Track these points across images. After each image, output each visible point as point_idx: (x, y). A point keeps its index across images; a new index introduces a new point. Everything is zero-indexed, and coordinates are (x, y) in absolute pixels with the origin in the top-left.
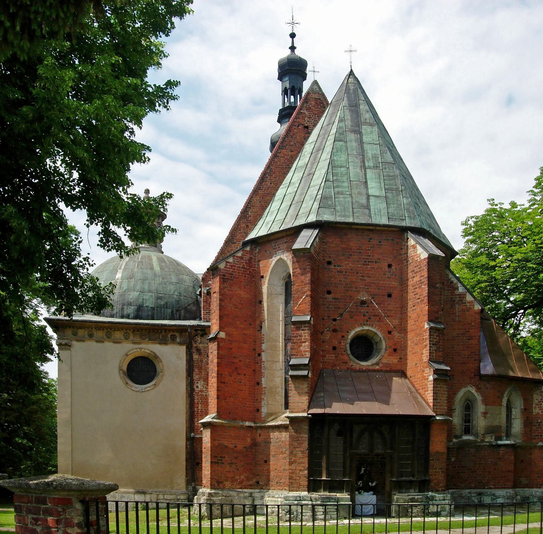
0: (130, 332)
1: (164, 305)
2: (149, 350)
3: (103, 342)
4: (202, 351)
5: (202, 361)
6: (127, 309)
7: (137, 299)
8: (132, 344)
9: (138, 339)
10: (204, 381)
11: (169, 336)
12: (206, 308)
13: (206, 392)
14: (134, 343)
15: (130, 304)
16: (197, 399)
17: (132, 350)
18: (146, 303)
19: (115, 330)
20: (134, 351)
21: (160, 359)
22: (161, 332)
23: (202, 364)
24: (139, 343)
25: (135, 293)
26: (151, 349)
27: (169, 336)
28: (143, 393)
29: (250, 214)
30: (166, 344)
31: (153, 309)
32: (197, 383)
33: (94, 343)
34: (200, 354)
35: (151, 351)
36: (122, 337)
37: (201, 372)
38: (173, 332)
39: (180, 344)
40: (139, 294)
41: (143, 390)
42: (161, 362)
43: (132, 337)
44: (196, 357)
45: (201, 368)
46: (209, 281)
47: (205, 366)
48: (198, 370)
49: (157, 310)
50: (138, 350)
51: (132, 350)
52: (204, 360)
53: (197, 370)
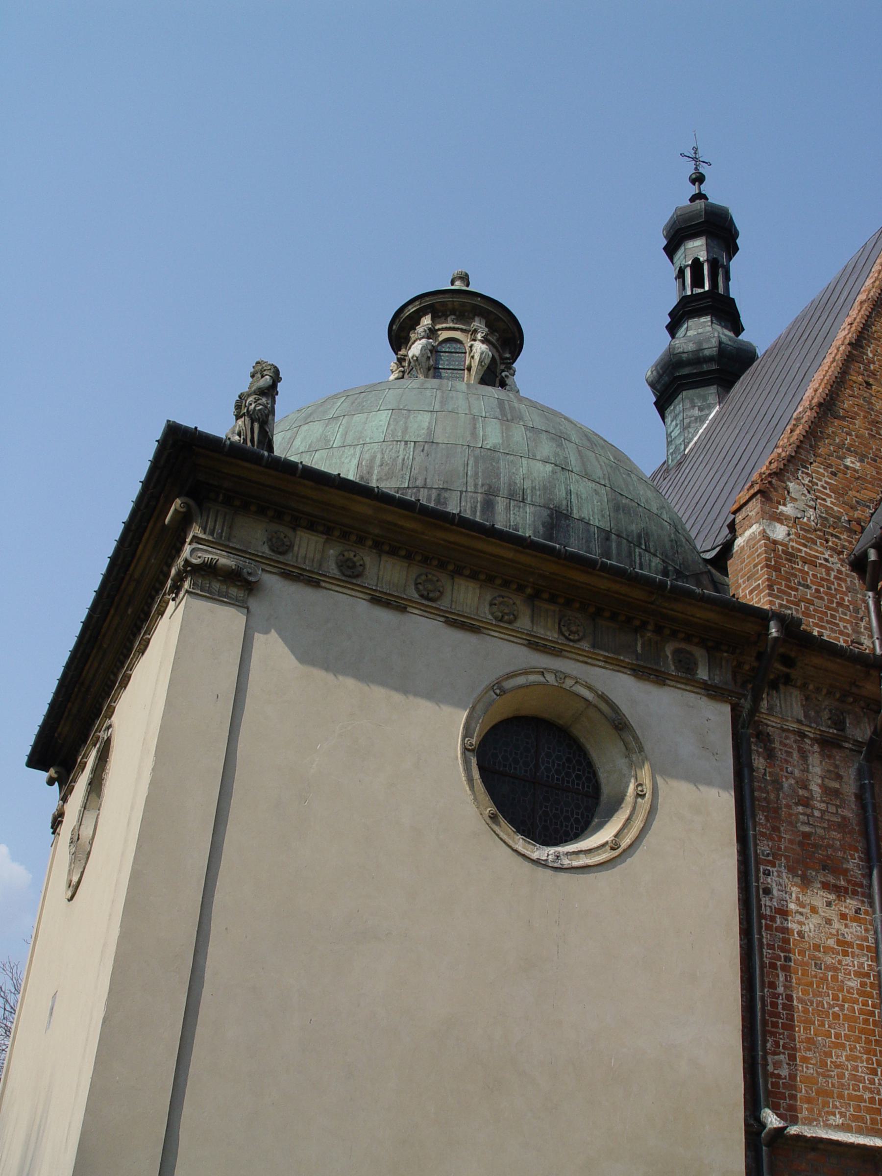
0: (518, 600)
1: (639, 536)
2: (590, 688)
3: (403, 609)
4: (777, 745)
5: (777, 784)
6: (508, 508)
7: (548, 488)
8: (524, 650)
9: (549, 633)
10: (791, 870)
11: (669, 650)
12: (779, 590)
13: (798, 917)
14: (535, 645)
15: (517, 496)
16: (771, 947)
17: (526, 672)
18: (580, 509)
19: (458, 572)
20: (533, 678)
21: (636, 739)
22: (644, 625)
23: (778, 799)
24: (555, 652)
25: (539, 465)
26: (601, 688)
27: (669, 653)
28: (563, 876)
29: (870, 355)
30: (659, 678)
31: (606, 535)
32: (767, 873)
33: (362, 606)
34: (770, 755)
35: (603, 697)
36: (485, 613)
37: (776, 829)
38: (688, 639)
39: (712, 692)
40: (554, 472)
41: (566, 862)
42: (641, 749)
43: (524, 623)
44: (759, 762)
45: (777, 810)
46: (779, 503)
47: (788, 806)
48: (767, 820)
49: (619, 545)
50: (551, 678)
51: (526, 672)
52: (786, 785)
53: (761, 818)
